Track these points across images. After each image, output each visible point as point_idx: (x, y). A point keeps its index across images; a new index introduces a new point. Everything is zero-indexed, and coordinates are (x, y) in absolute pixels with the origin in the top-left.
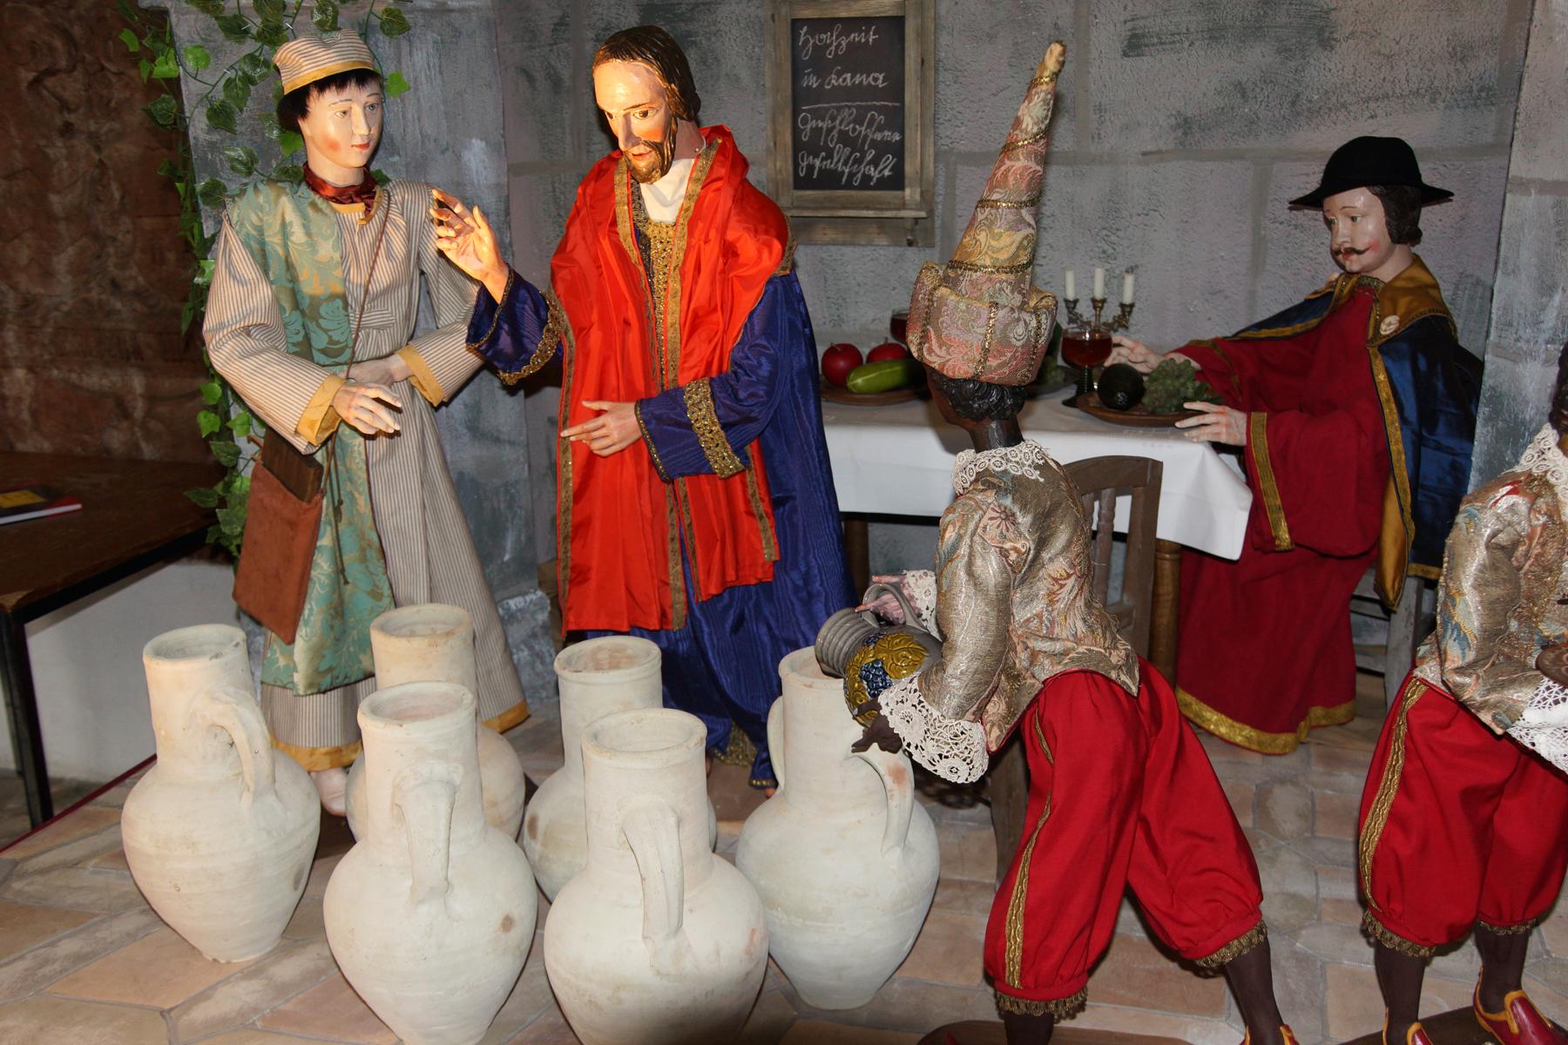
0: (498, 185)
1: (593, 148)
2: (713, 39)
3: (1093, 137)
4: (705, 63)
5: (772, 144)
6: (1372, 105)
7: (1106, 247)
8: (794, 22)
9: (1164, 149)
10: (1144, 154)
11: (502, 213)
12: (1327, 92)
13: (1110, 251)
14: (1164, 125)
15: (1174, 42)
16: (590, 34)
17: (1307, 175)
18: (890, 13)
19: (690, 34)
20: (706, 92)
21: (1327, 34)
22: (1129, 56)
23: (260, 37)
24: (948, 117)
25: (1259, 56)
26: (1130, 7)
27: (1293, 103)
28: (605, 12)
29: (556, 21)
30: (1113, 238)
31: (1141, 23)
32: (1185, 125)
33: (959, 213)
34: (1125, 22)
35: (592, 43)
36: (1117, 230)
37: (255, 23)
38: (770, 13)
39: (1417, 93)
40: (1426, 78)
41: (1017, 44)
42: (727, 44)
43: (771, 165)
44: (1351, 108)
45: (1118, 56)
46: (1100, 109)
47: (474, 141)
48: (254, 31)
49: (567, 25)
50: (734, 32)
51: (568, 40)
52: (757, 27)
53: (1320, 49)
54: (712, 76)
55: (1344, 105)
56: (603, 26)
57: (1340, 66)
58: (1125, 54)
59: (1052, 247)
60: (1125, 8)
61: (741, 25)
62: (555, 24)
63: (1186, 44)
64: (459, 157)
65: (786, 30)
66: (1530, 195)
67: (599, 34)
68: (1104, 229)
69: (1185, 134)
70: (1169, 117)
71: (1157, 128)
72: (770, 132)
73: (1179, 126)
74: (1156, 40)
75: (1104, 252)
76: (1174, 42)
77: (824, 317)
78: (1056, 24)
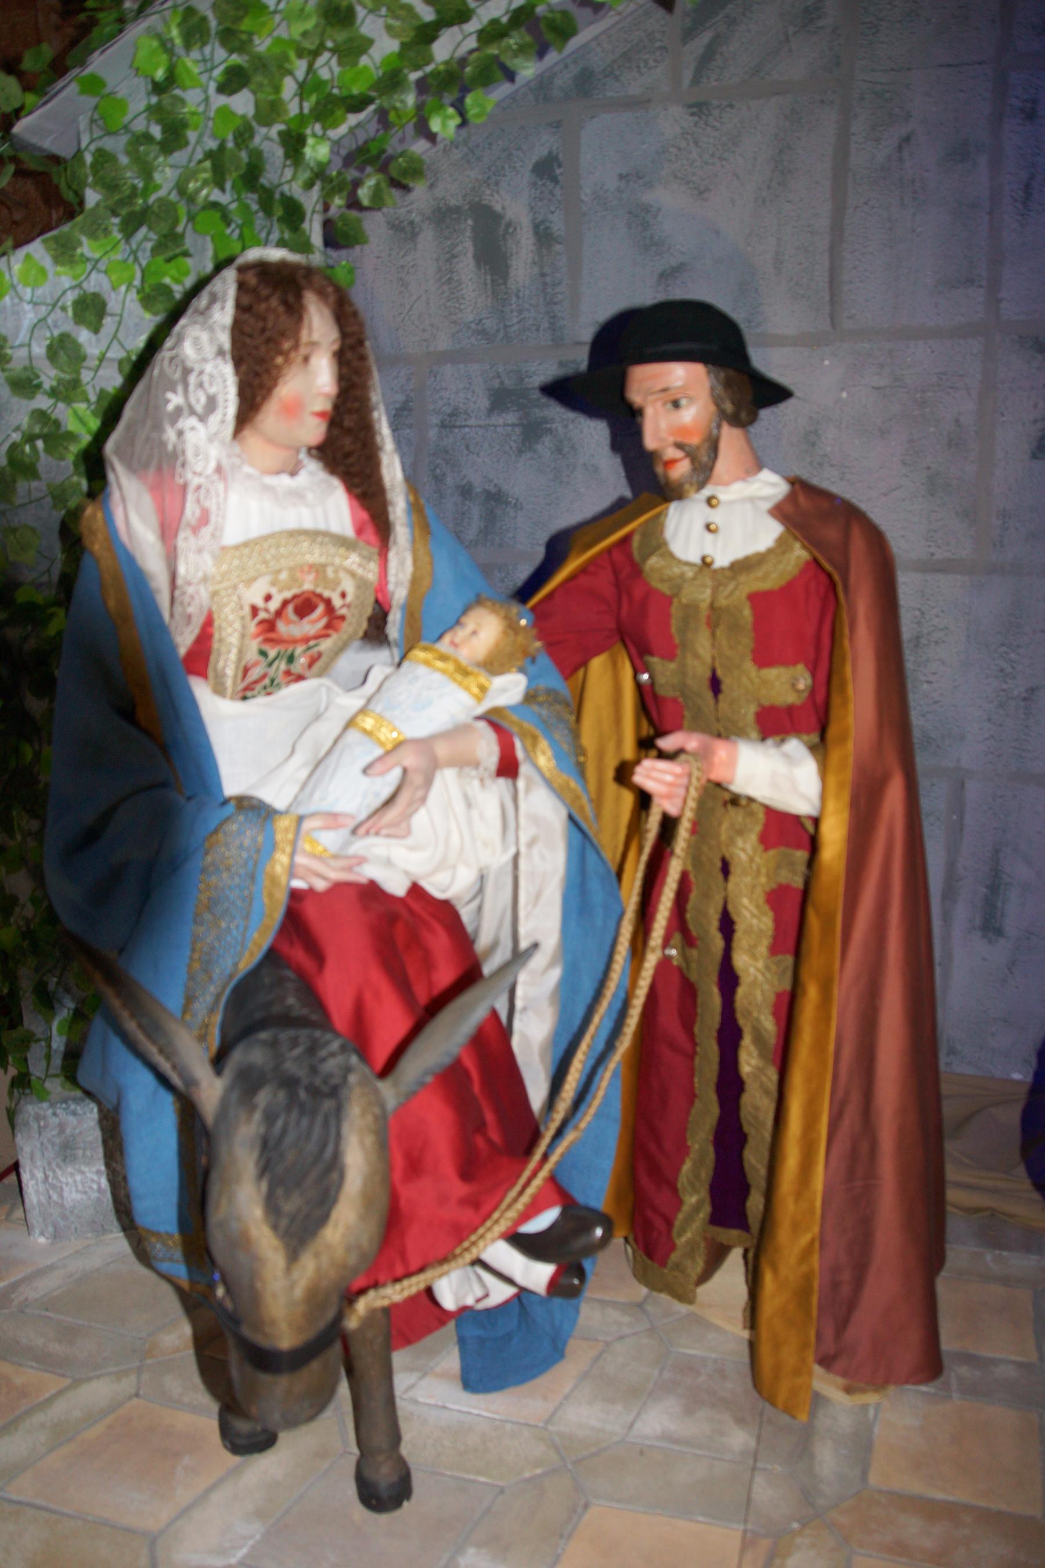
2: (571, 426)
4: (559, 450)
7: (1005, 665)
13: (1009, 670)
16: (435, 420)
19: (545, 420)
20: (561, 483)
23: (54, 393)
29: (398, 406)
30: (1012, 655)
36: (1018, 646)
37: (49, 376)
48: (47, 386)
49: (411, 410)
51: (410, 426)
54: (568, 466)
56: (449, 411)
58: (1034, 456)
59: (943, 663)
62: (397, 410)
67: (445, 420)
68: (1003, 645)
75: (1002, 670)
78: (957, 421)
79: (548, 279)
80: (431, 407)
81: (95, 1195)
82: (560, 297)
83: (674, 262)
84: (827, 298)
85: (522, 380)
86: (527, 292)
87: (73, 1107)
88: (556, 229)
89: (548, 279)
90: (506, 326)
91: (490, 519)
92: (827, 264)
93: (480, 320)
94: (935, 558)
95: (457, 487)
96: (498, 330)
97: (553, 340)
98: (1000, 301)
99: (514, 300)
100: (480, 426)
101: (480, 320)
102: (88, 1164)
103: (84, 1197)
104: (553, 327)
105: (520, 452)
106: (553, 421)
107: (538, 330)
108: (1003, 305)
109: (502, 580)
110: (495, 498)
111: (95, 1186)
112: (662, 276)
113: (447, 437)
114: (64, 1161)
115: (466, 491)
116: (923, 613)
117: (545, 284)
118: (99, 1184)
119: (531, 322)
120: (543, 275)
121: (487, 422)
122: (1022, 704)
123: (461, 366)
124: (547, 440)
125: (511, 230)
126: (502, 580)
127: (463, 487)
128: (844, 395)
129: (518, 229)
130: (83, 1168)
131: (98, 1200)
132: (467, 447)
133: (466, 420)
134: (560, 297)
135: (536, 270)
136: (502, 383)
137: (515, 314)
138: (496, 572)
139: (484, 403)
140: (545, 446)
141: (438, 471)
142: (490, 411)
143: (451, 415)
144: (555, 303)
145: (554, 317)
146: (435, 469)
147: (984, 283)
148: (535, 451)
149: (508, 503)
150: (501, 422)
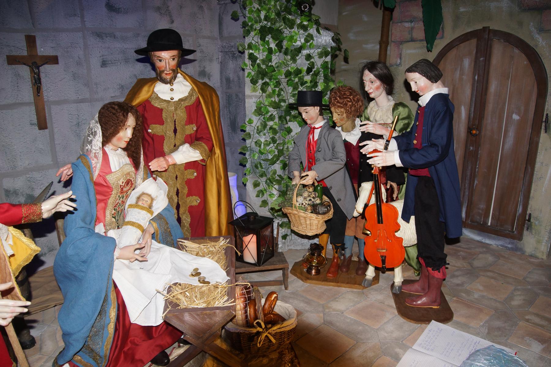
3: (95, 93)
14: (116, 88)
15: (115, 63)
24: (45, 89)
26: (101, 52)
33: (54, 122)
34: (100, 57)
45: (100, 67)
46: (96, 84)
58: (102, 67)
60: (100, 52)
63: (119, 63)
66: (253, 99)
69: (122, 90)
70: (117, 85)
76: (115, 63)
77: (8, 167)
78: (79, 57)
94: (79, 98)
98: (85, 21)
108: (86, 23)
116: (78, 116)
128: (42, 49)
147: (80, 16)
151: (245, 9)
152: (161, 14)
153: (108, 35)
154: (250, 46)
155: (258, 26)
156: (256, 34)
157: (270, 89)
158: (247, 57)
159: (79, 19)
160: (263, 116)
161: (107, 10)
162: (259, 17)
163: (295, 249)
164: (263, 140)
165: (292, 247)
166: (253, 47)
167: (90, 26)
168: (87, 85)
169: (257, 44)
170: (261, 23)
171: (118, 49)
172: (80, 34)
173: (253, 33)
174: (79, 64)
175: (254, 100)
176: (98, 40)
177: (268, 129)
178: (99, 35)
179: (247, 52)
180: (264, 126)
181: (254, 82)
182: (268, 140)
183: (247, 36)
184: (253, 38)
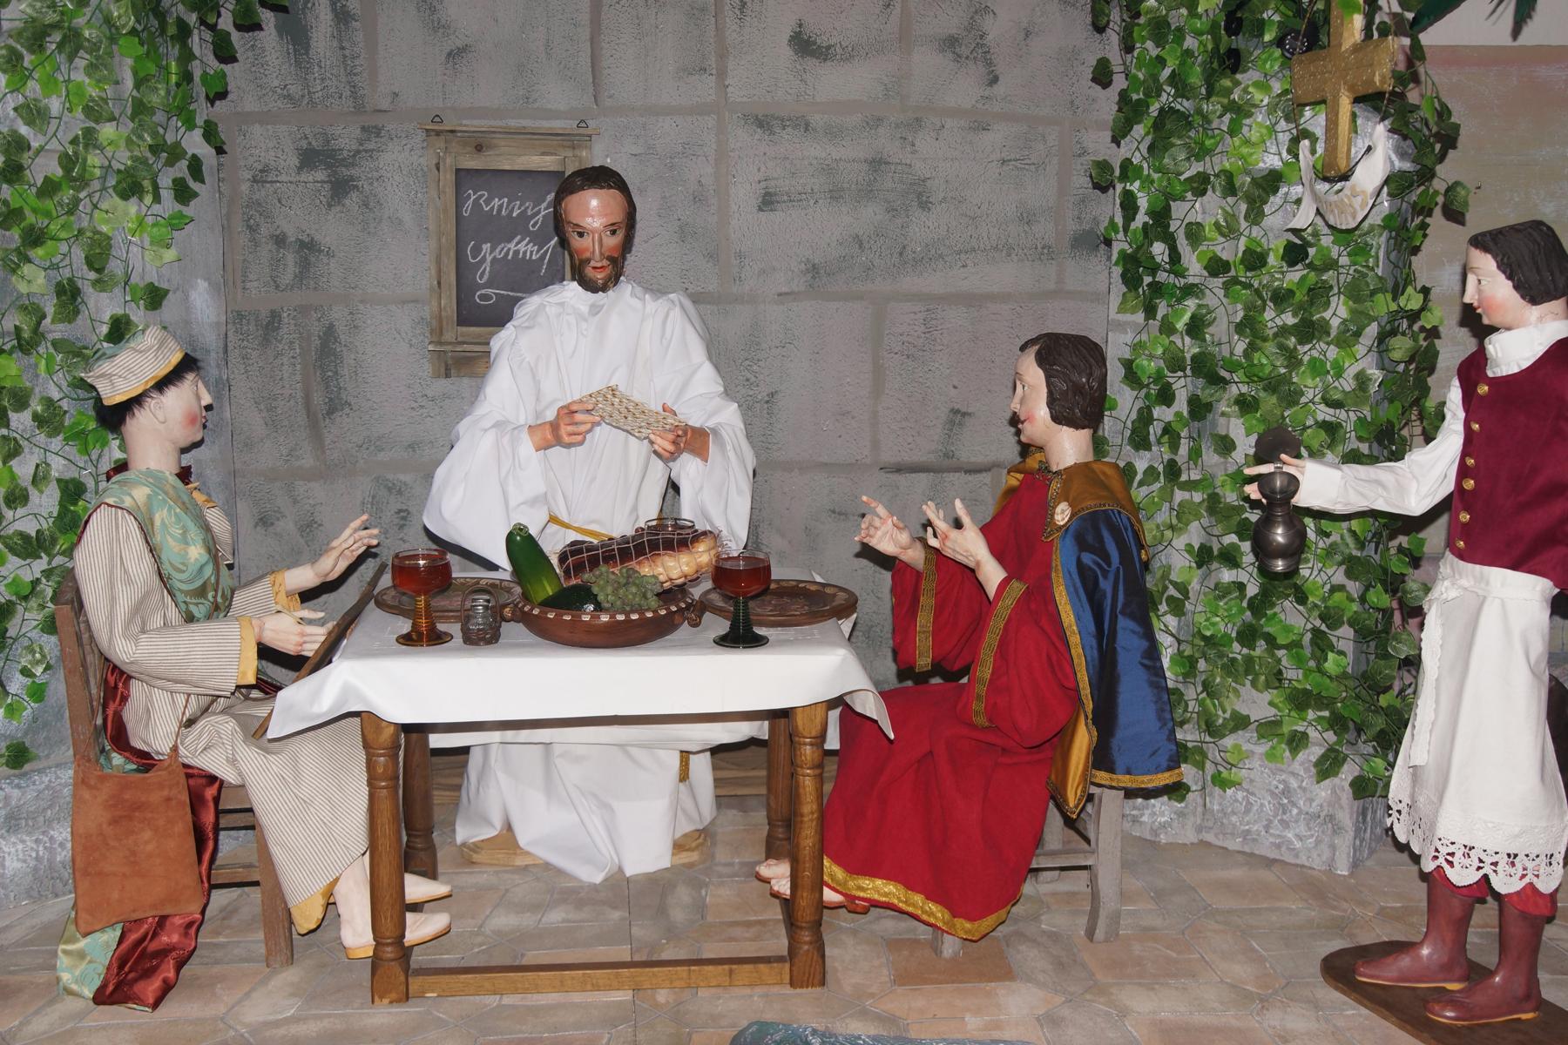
0: (218, 324)
1: (248, 285)
2: (375, 184)
4: (366, 205)
5: (436, 283)
6: (963, 256)
7: (749, 376)
8: (458, 171)
9: (796, 290)
10: (780, 295)
11: (221, 351)
12: (927, 245)
13: (753, 379)
14: (796, 270)
16: (248, 175)
17: (915, 313)
18: (552, 169)
21: (924, 198)
22: (763, 211)
25: (871, 214)
26: (763, 169)
27: (901, 254)
28: (263, 154)
31: (772, 183)
32: (814, 270)
34: (760, 182)
35: (248, 184)
38: (434, 162)
39: (996, 248)
40: (1003, 237)
41: (665, 197)
42: (389, 188)
43: (435, 303)
44: (946, 258)
45: (755, 210)
46: (740, 255)
47: (199, 281)
50: (396, 178)
52: (419, 174)
53: (920, 210)
55: (941, 256)
56: (260, 167)
57: (936, 224)
58: (760, 209)
60: (759, 170)
61: (404, 172)
63: (812, 202)
64: (187, 298)
65: (448, 178)
69: (813, 277)
71: (790, 273)
72: (433, 272)
73: (808, 271)
74: (786, 198)
75: (748, 380)
79: (347, 52)
80: (242, 163)
81: (32, 863)
82: (359, 69)
83: (459, 44)
84: (591, 80)
85: (328, 142)
86: (328, 63)
87: (16, 781)
88: (352, 7)
89: (347, 52)
90: (309, 93)
91: (305, 266)
92: (589, 50)
93: (285, 86)
95: (272, 237)
96: (303, 96)
97: (355, 107)
99: (316, 69)
100: (291, 182)
101: (285, 86)
102: (29, 834)
103: (24, 865)
104: (354, 96)
105: (330, 206)
106: (359, 179)
107: (340, 98)
108: (730, 89)
109: (319, 320)
110: (308, 248)
111: (34, 855)
112: (449, 54)
113: (259, 190)
114: (8, 831)
115: (280, 240)
117: (345, 56)
118: (37, 852)
119: (333, 90)
120: (343, 48)
121: (298, 178)
122: (766, 406)
123: (269, 127)
124: (354, 195)
125: (309, 5)
126: (319, 320)
127: (277, 236)
129: (317, 4)
130: (24, 837)
131: (36, 869)
132: (280, 202)
133: (277, 175)
134: (359, 69)
135: (335, 43)
136: (310, 143)
137: (318, 81)
138: (313, 312)
139: (294, 161)
140: (353, 200)
141: (252, 221)
142: (300, 169)
143: (261, 171)
144: (355, 75)
145: (354, 87)
146: (249, 219)
147: (714, 72)
148: (343, 205)
149: (320, 251)
150: (311, 178)
151: (1129, 49)
152: (959, 56)
153: (788, 123)
154: (1126, 164)
155: (1154, 109)
156: (1147, 134)
157: (1162, 309)
158: (1118, 201)
159: (711, 81)
160: (1144, 391)
161: (792, 53)
162: (1155, 78)
163: (1219, 843)
164: (1141, 465)
165: (1209, 837)
166: (1130, 174)
167: (739, 100)
168: (713, 256)
169: (1145, 166)
170: (1159, 95)
171: (815, 162)
172: (711, 121)
173: (1139, 130)
174: (698, 199)
175: (1129, 337)
176: (757, 137)
177: (1159, 432)
178: (763, 123)
179: (1119, 187)
180: (1145, 418)
181: (1131, 280)
182: (1156, 466)
183: (1124, 136)
184: (1139, 143)
